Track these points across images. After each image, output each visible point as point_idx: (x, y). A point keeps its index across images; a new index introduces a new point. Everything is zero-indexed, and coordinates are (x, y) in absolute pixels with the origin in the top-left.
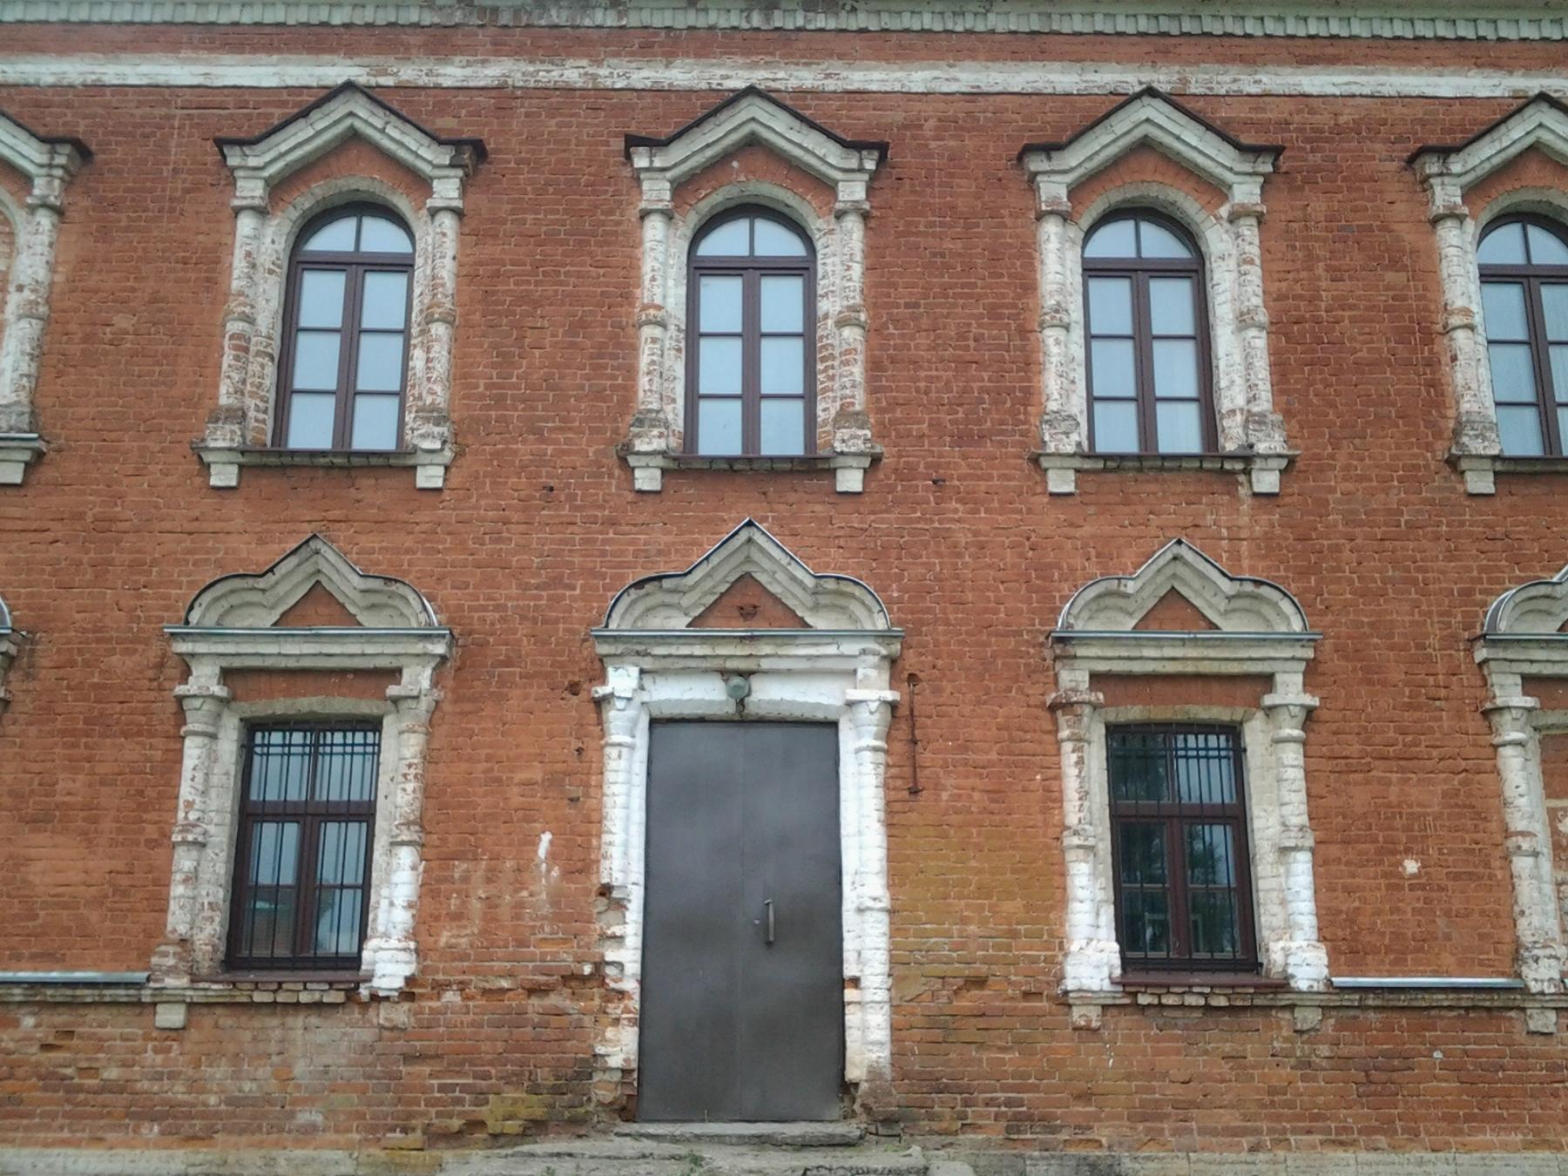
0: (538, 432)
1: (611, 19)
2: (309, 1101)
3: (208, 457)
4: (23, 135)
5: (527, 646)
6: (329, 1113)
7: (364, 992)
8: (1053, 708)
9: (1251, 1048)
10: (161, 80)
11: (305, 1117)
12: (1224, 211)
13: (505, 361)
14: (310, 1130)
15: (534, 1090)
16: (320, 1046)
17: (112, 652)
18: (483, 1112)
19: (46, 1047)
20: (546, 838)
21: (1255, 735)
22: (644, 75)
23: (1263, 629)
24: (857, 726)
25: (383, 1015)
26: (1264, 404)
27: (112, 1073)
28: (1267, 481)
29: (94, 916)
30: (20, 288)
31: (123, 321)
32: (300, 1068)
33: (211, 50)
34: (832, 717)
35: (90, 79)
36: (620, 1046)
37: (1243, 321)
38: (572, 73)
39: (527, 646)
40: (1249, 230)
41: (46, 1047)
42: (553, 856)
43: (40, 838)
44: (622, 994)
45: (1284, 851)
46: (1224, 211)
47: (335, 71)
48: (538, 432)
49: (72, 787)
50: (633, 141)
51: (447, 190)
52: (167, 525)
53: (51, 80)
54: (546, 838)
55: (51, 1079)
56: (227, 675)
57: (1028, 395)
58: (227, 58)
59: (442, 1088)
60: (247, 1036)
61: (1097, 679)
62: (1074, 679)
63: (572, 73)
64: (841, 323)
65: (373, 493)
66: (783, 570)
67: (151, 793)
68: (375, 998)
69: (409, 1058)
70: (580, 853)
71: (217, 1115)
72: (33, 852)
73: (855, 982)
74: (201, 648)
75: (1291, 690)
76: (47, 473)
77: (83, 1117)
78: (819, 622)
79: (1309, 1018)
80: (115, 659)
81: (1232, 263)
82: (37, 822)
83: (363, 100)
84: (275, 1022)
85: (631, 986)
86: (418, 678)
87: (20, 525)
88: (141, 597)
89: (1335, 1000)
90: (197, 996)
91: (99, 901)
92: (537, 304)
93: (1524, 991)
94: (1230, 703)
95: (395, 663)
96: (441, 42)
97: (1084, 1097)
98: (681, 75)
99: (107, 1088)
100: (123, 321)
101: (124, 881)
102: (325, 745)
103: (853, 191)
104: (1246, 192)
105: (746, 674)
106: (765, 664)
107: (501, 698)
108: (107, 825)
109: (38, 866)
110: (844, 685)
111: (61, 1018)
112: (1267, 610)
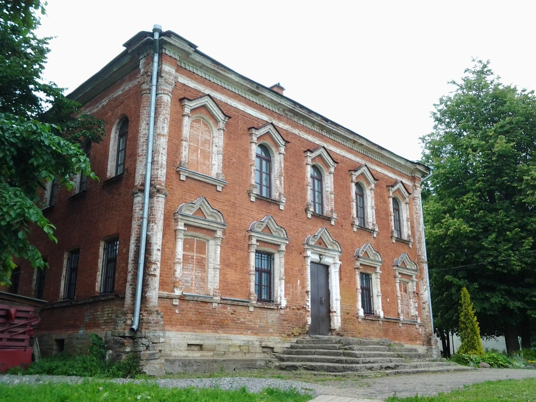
0: (294, 202)
1: (302, 123)
2: (271, 328)
3: (252, 194)
4: (221, 112)
5: (295, 244)
6: (273, 330)
7: (279, 307)
8: (355, 268)
9: (375, 326)
10: (237, 107)
11: (271, 330)
12: (369, 188)
13: (289, 187)
14: (271, 333)
15: (299, 328)
16: (272, 317)
17: (237, 232)
18: (293, 331)
19: (232, 314)
20: (299, 281)
21: (373, 276)
22: (306, 136)
23: (376, 259)
24: (335, 267)
25: (282, 312)
26: (375, 223)
27: (242, 320)
28: (375, 235)
29: (238, 287)
30: (216, 146)
31: (234, 160)
32: (269, 321)
33: (246, 104)
34: (328, 264)
35: (226, 102)
36: (309, 320)
37: (372, 208)
38: (296, 131)
39: (295, 244)
40: (373, 192)
41: (232, 314)
42: (300, 284)
43: (228, 270)
44: (308, 311)
45: (378, 296)
46: (369, 188)
47: (265, 117)
48: (294, 202)
49: (232, 259)
50: (309, 150)
51: (282, 150)
52: (244, 207)
53: (219, 99)
54: (299, 281)
55: (233, 320)
56: (257, 241)
57: (350, 213)
58: (248, 107)
59: (289, 326)
60: (261, 314)
61: (361, 265)
62: (358, 264)
63: (296, 131)
64: (331, 193)
65: (273, 208)
66: (328, 239)
67: (245, 263)
68: (281, 308)
69: (284, 320)
71: (258, 330)
72: (227, 272)
73: (335, 312)
74: (256, 235)
76: (224, 190)
77: (238, 328)
78: (329, 247)
79: (381, 322)
80: (238, 234)
81: (370, 197)
82: (228, 266)
83: (272, 127)
84: (265, 312)
85: (310, 310)
86: (283, 248)
87: (221, 201)
88: (241, 221)
89: (385, 320)
90: (256, 305)
91: (238, 284)
92: (294, 176)
93: (399, 320)
94: (371, 271)
95: (279, 243)
96: (280, 117)
97: (359, 333)
98: (310, 138)
99: (242, 323)
100: (234, 160)
101: (242, 280)
102: (261, 257)
103: (332, 170)
104: (373, 186)
105: (321, 255)
106: (326, 254)
107: (292, 253)
108: (239, 268)
109: (228, 276)
111: (234, 308)
112: (376, 257)
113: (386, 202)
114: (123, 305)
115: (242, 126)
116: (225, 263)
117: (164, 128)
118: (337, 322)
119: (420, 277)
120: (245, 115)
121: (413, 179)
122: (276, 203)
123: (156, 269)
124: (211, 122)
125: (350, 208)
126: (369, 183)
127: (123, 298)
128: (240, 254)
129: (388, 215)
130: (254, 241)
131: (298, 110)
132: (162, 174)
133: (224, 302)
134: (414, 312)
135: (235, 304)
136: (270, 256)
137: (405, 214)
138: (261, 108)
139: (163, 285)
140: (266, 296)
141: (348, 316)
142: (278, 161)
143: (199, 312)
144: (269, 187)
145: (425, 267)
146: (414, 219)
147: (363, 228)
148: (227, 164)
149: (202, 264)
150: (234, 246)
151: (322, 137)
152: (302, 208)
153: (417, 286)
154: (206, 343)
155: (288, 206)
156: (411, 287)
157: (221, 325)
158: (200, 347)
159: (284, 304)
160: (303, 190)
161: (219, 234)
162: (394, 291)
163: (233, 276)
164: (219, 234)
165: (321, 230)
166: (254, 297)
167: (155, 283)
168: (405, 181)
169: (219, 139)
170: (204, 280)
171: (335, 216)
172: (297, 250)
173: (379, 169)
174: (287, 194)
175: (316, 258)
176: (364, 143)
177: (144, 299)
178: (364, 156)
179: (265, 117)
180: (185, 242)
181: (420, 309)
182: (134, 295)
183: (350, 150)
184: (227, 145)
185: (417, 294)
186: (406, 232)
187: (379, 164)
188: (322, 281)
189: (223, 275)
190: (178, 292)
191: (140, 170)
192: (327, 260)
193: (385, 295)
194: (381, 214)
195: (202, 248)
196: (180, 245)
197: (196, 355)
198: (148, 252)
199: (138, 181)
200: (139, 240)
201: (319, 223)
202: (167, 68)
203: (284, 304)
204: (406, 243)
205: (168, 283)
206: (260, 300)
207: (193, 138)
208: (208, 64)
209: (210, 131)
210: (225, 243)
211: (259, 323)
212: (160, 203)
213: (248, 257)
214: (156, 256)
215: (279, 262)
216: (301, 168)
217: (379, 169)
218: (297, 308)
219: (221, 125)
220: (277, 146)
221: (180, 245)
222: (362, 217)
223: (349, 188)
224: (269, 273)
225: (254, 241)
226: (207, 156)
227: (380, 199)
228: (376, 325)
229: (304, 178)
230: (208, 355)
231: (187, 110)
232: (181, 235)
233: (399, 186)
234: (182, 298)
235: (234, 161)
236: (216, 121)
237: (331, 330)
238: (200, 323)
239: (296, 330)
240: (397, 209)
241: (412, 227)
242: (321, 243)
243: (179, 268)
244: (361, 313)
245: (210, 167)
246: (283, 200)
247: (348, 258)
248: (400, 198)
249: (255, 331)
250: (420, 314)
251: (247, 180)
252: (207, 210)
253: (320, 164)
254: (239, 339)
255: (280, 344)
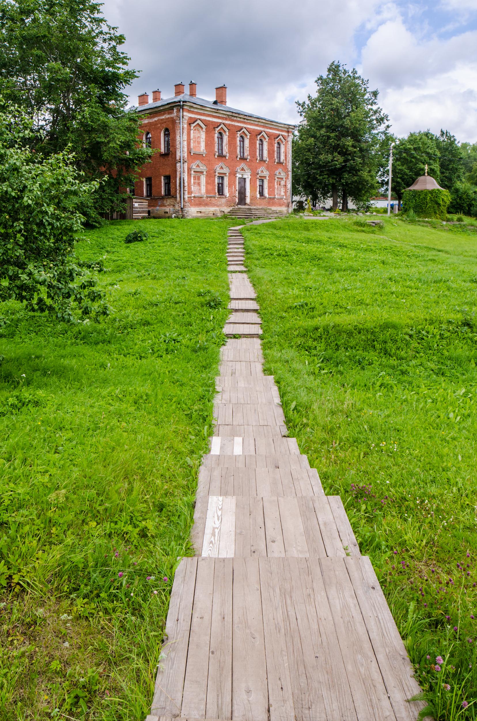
21: (265, 180)
23: (266, 173)
36: (237, 201)
38: (233, 123)
47: (220, 121)
51: (227, 133)
63: (233, 123)
65: (224, 159)
66: (245, 168)
70: (235, 188)
75: (267, 178)
86: (227, 174)
96: (226, 119)
103: (248, 137)
110: (247, 176)
113: (273, 146)
114: (176, 200)
115: (211, 127)
116: (207, 183)
117: (185, 137)
118: (248, 201)
119: (287, 178)
120: (212, 122)
121: (288, 132)
122: (225, 157)
123: (186, 188)
124: (200, 129)
125: (256, 152)
126: (265, 139)
127: (176, 198)
128: (212, 179)
129: (274, 152)
130: (217, 174)
131: (234, 115)
132: (186, 155)
133: (207, 197)
134: (283, 194)
135: (211, 197)
136: (222, 178)
137: (283, 149)
138: (219, 117)
139: (189, 193)
140: (221, 191)
141: (253, 198)
142: (226, 138)
143: (199, 201)
144: (222, 150)
145: (290, 174)
146: (286, 153)
147: (262, 160)
148: (207, 145)
149: (199, 184)
150: (210, 176)
151: (244, 123)
152: (235, 156)
153: (286, 182)
154: (202, 211)
155: (230, 157)
156: (283, 183)
157: (206, 205)
158: (201, 212)
159: (228, 195)
160: (236, 148)
161: (205, 173)
162: (274, 186)
163: (210, 187)
164: (205, 173)
165: (243, 165)
166: (217, 194)
167: (186, 193)
168: (284, 133)
169: (203, 135)
170: (200, 190)
171: (249, 157)
172: (233, 174)
173: (271, 131)
174: (230, 152)
175: (241, 176)
176: (264, 121)
177: (184, 198)
178: (263, 127)
179: (220, 121)
180: (194, 177)
181: (286, 192)
182: (180, 197)
183: (257, 125)
184: (206, 137)
185: (285, 186)
186: (282, 158)
187: (271, 128)
188: (243, 185)
189: (206, 187)
190: (193, 195)
191: (178, 154)
192: (245, 176)
193: (269, 187)
194: (271, 153)
195: (199, 178)
196: (192, 178)
197: (200, 215)
198: (184, 183)
199: (178, 158)
200: (180, 179)
201: (242, 161)
202: (185, 114)
203: (228, 195)
204: (282, 163)
205: (190, 193)
206: (219, 195)
207: (194, 137)
208: (199, 107)
209: (199, 133)
210: (207, 176)
211: (219, 203)
212: (186, 165)
213: (215, 180)
214: (186, 184)
215: (226, 180)
216: (235, 139)
217: (271, 131)
218: (232, 196)
219: (204, 130)
220: (225, 132)
221: (192, 178)
222: (262, 155)
223: (256, 143)
224: (222, 184)
225: (217, 174)
226: (199, 143)
227: (271, 145)
228: (265, 200)
229: (236, 143)
230: (202, 214)
231: (192, 128)
232: (192, 176)
233: (281, 137)
234: (194, 197)
235: (209, 144)
236: (202, 128)
237: (245, 204)
238: (199, 204)
239: (232, 204)
240: (279, 148)
241: (286, 155)
242: (243, 169)
243: (192, 187)
244: (258, 196)
245: (200, 147)
246: (228, 155)
247: (254, 174)
248: (280, 142)
249: (218, 206)
250: (286, 195)
251: (214, 150)
252: (200, 165)
253: (243, 135)
254: (212, 209)
255: (227, 210)
